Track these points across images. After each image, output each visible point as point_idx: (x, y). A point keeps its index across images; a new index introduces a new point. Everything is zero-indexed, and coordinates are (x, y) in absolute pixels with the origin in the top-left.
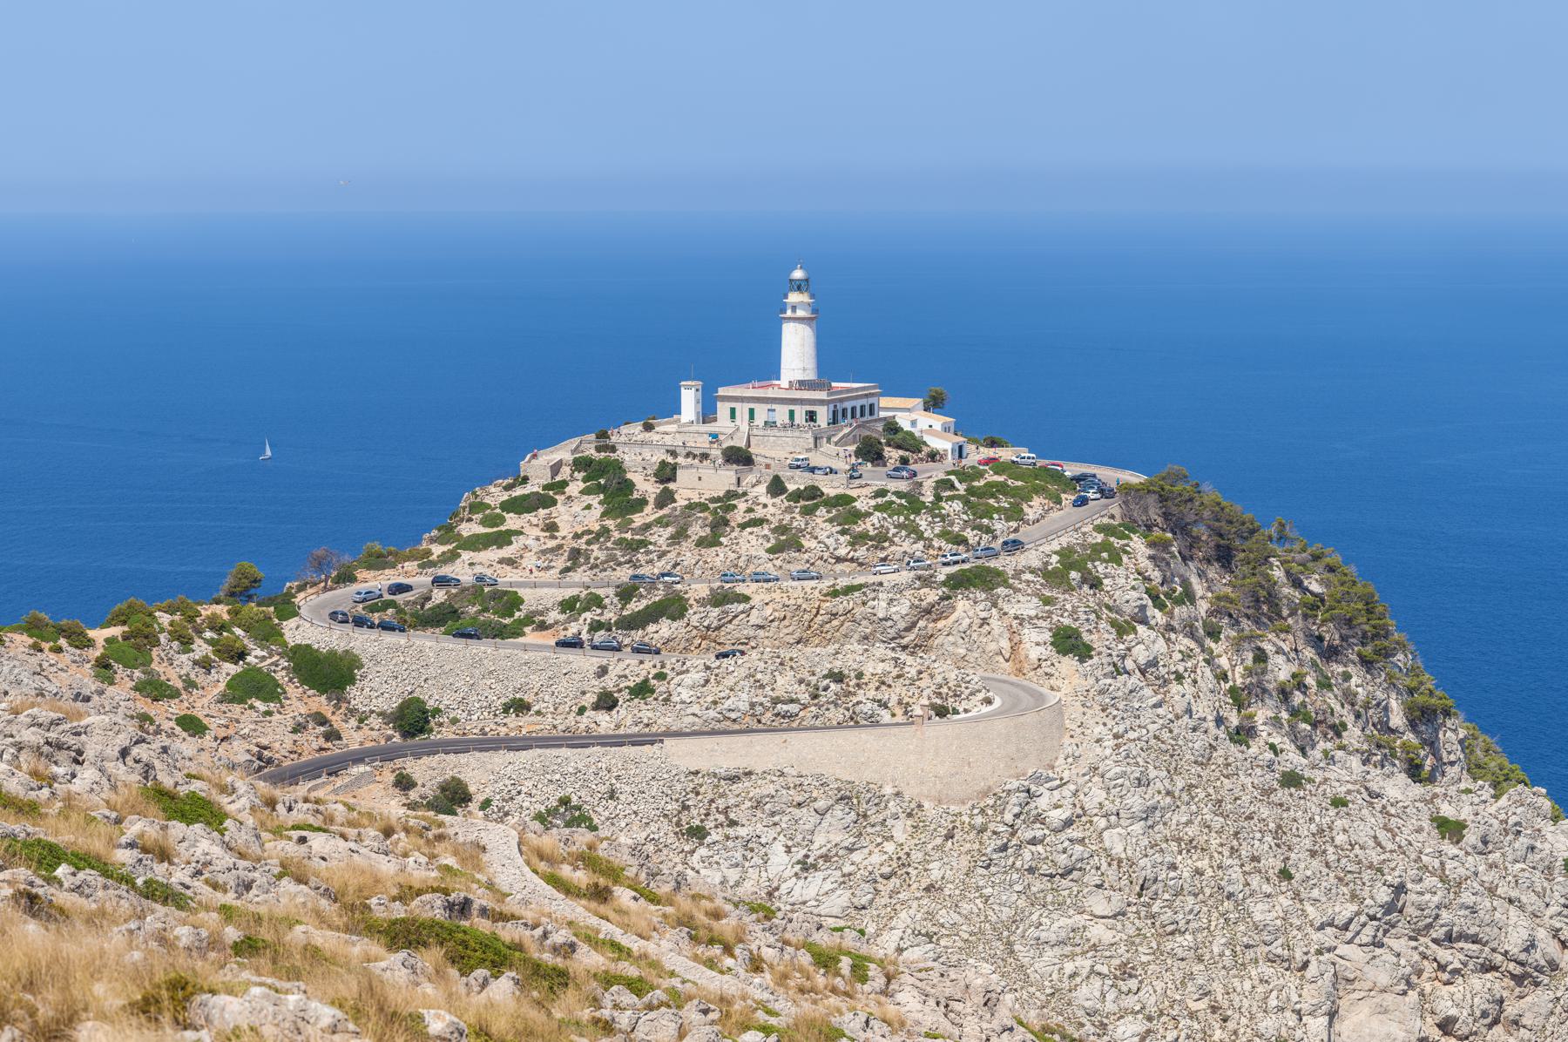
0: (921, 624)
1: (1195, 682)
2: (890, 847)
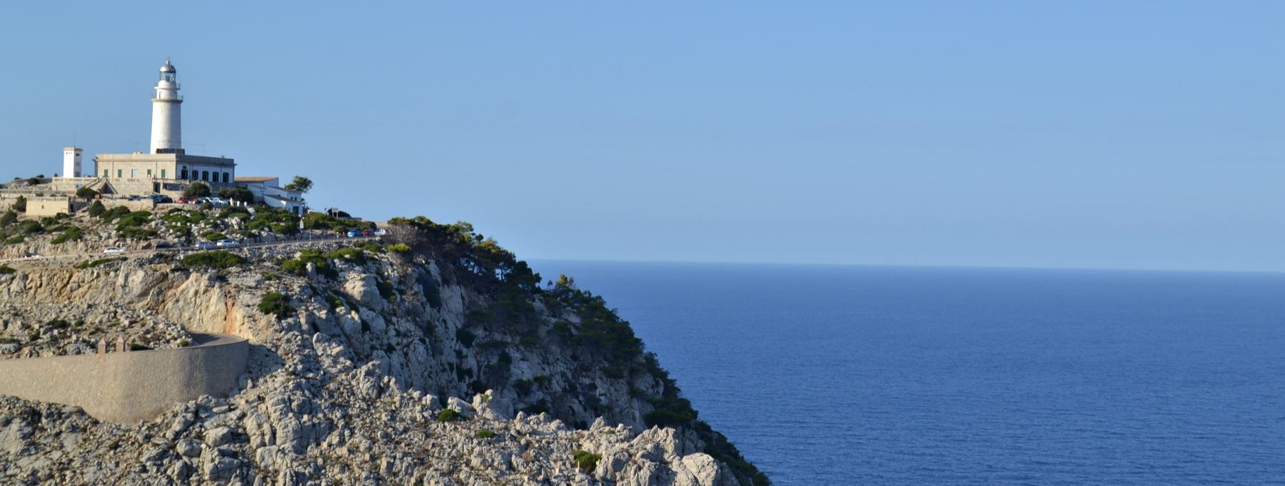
1: (406, 354)
2: (56, 455)
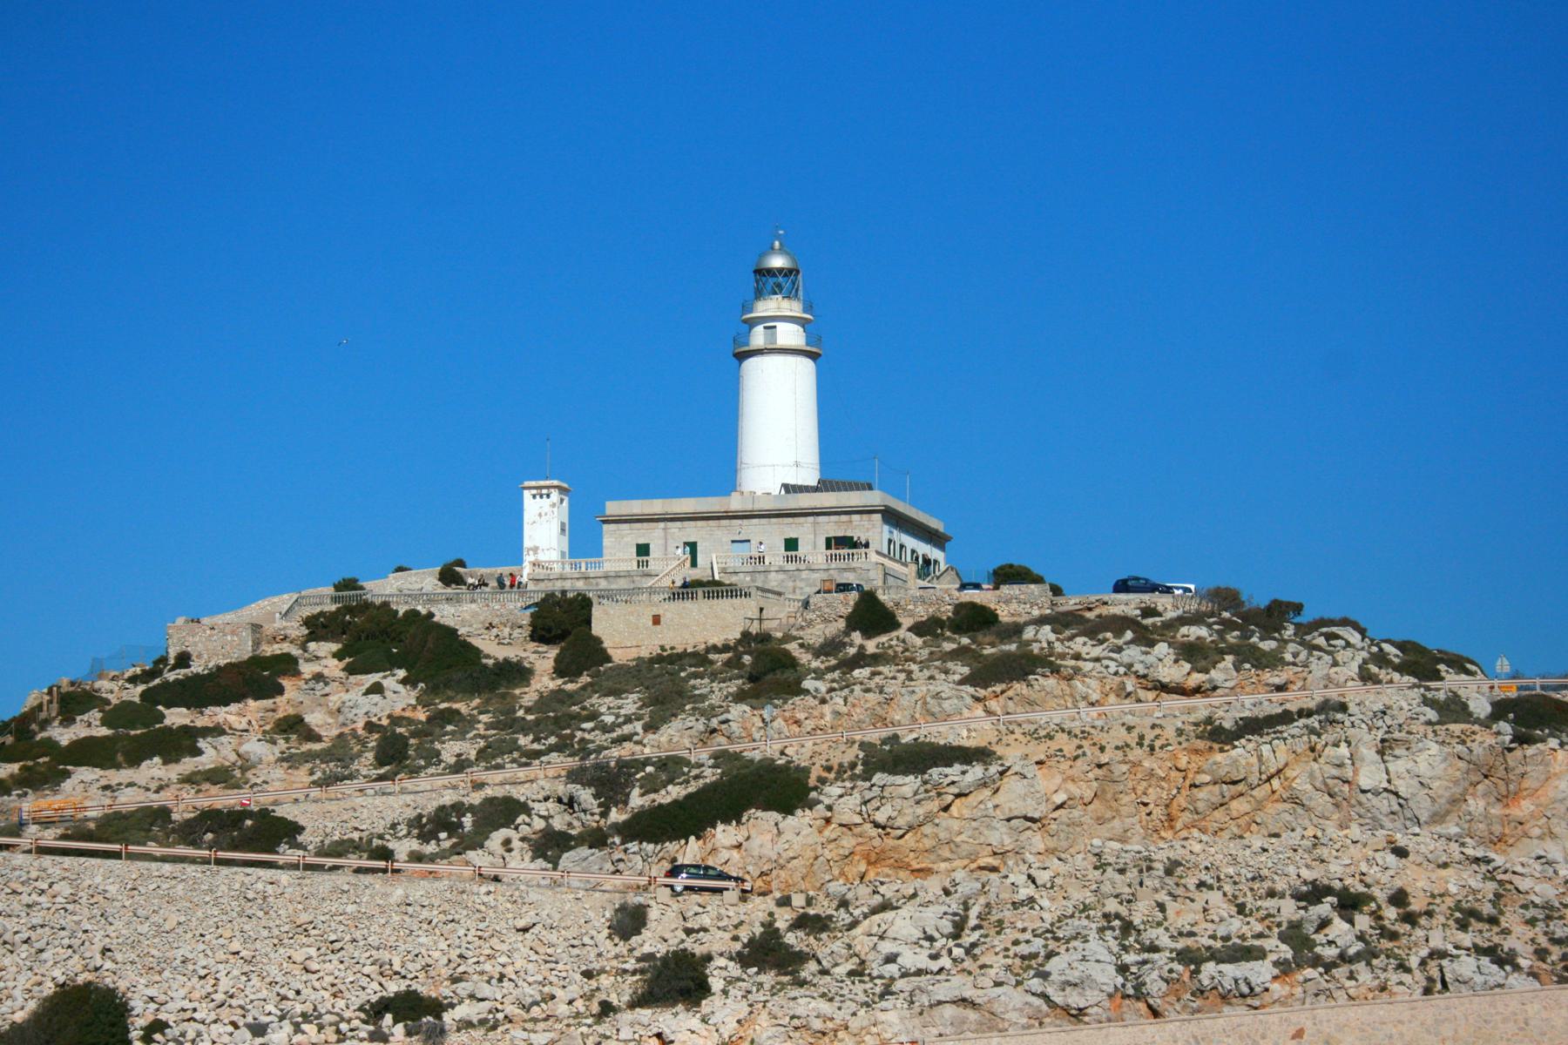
0: (1476, 805)
